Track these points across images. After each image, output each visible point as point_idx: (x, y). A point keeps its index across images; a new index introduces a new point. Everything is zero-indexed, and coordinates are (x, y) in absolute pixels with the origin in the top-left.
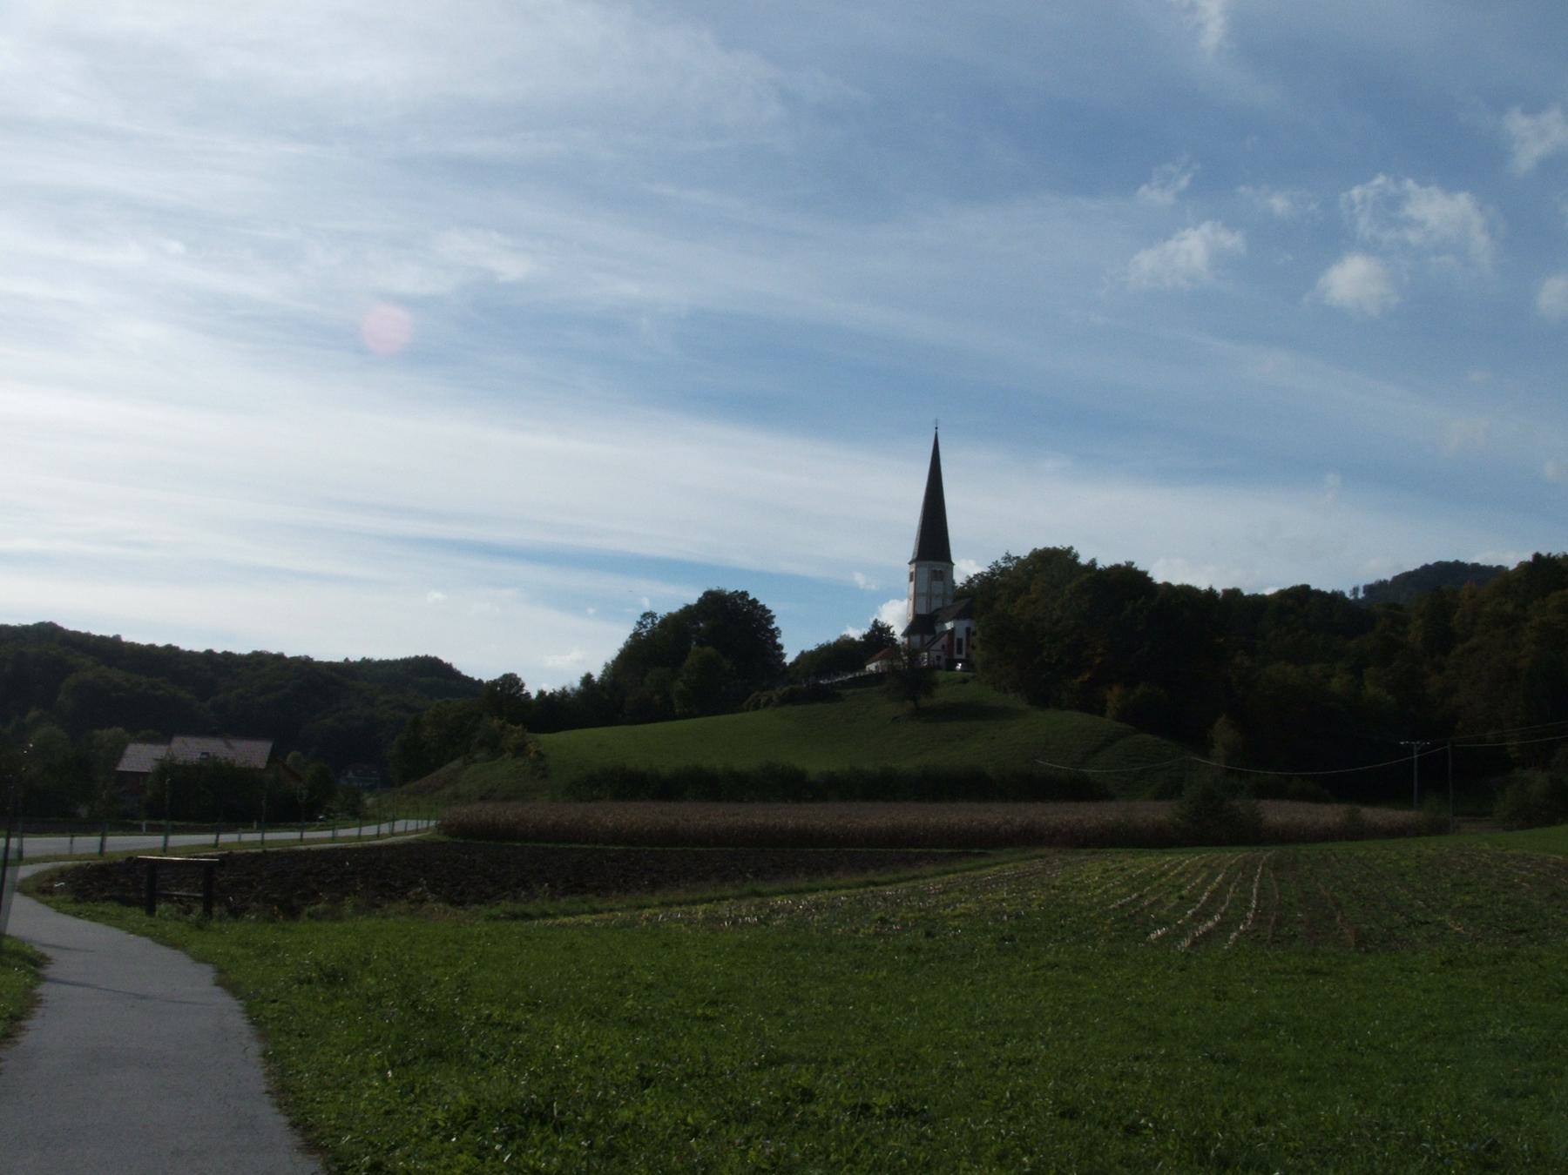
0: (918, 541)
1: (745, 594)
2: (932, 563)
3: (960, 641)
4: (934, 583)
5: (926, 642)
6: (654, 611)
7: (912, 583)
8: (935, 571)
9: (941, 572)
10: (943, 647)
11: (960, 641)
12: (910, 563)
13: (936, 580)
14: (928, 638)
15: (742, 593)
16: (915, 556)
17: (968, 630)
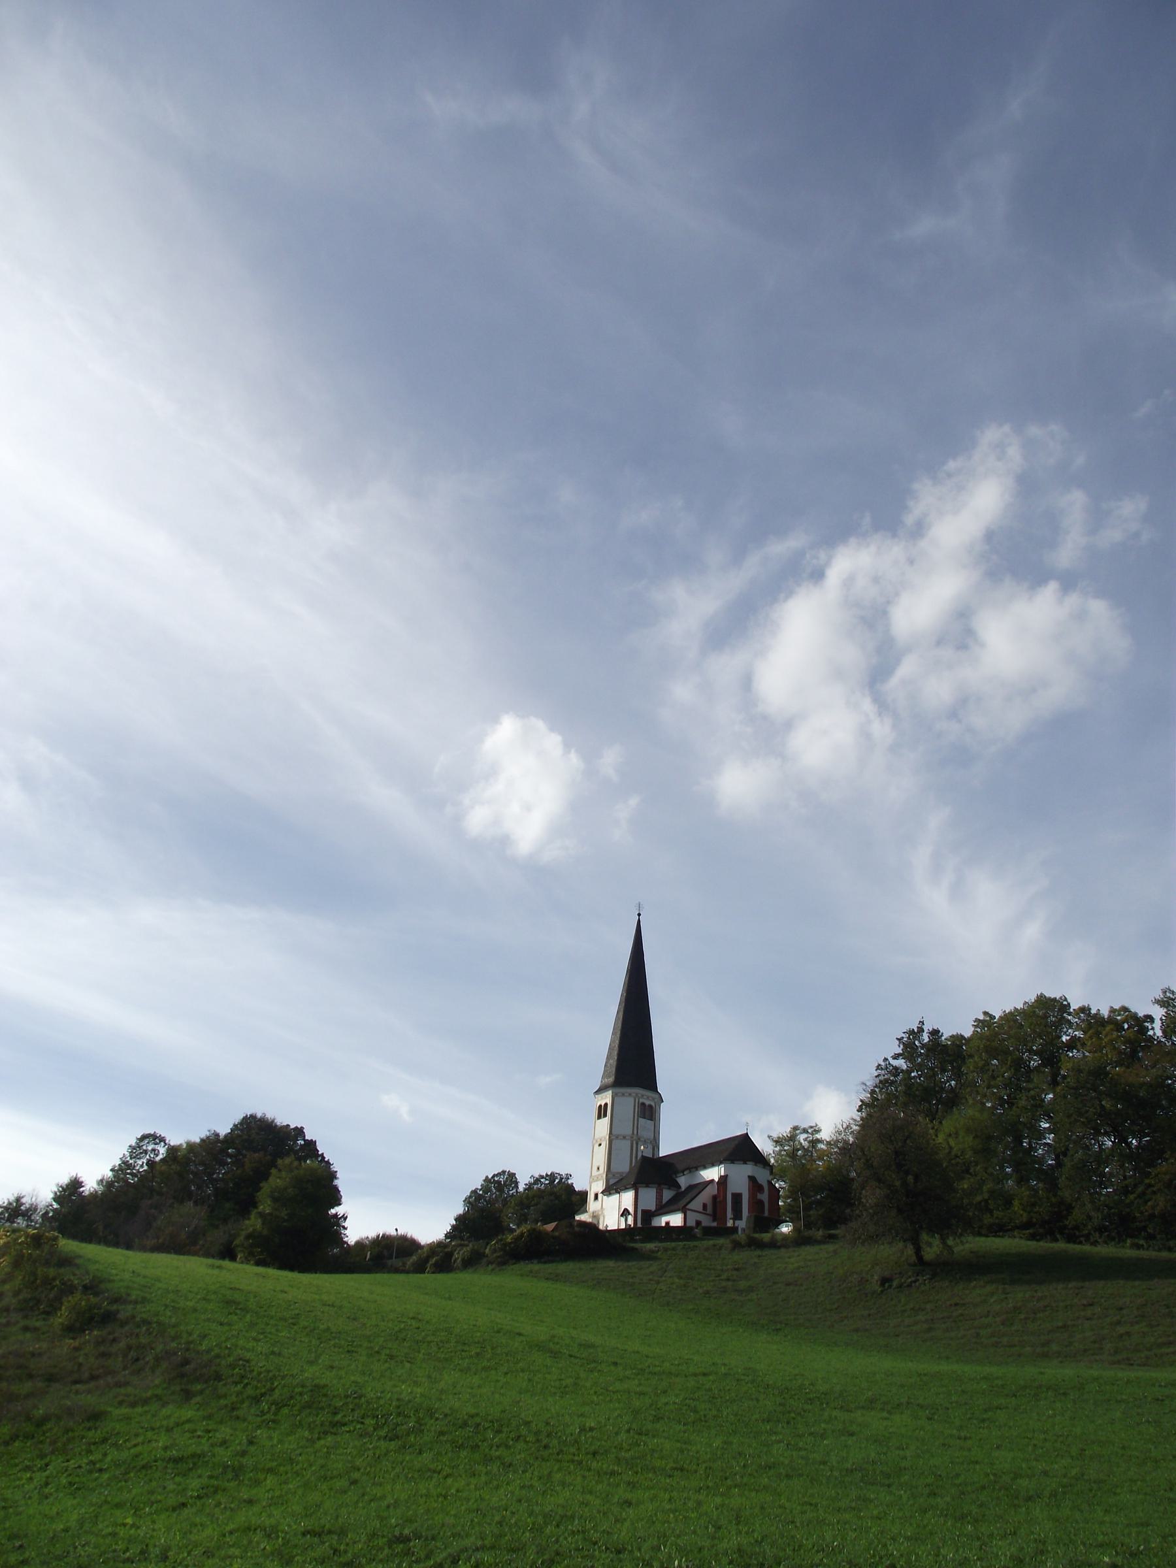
0: (613, 1062)
1: (300, 1131)
2: (640, 1091)
3: (737, 1197)
4: (640, 1119)
5: (664, 1202)
6: (161, 1132)
7: (605, 1121)
8: (643, 1104)
9: (650, 1106)
10: (705, 1206)
11: (737, 1197)
12: (598, 1092)
13: (645, 1118)
14: (668, 1194)
15: (296, 1128)
16: (611, 1080)
17: (752, 1179)
